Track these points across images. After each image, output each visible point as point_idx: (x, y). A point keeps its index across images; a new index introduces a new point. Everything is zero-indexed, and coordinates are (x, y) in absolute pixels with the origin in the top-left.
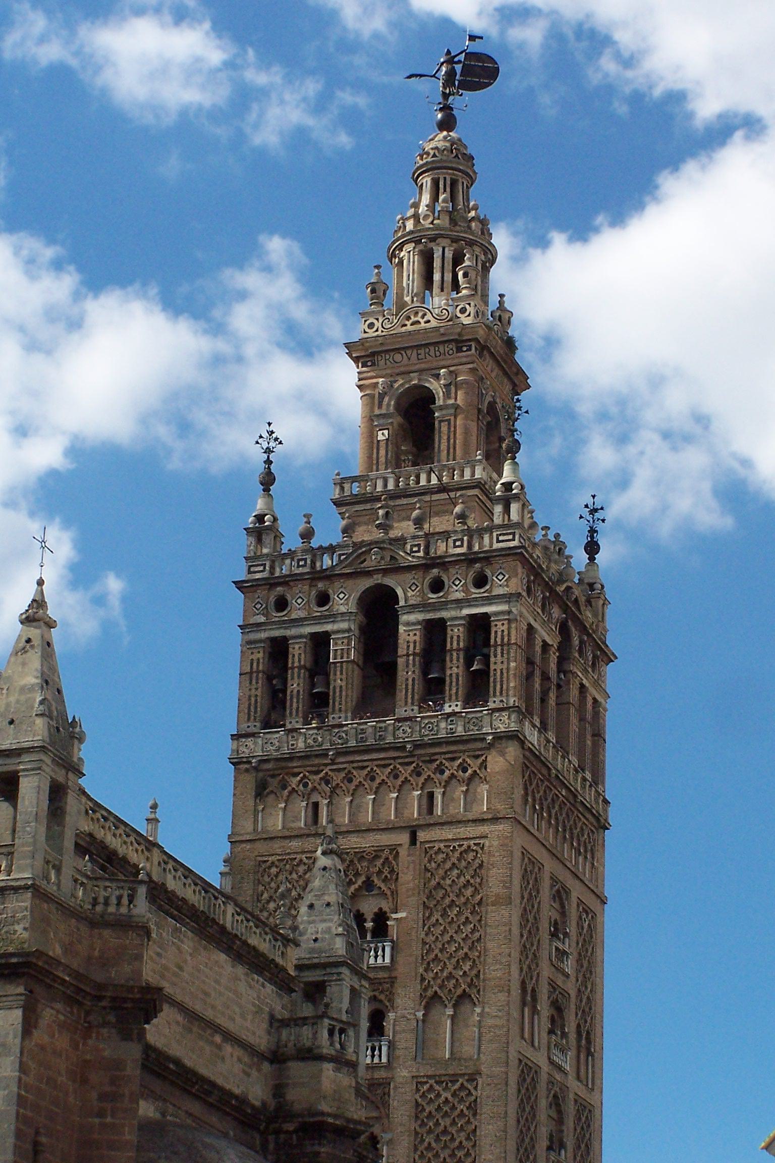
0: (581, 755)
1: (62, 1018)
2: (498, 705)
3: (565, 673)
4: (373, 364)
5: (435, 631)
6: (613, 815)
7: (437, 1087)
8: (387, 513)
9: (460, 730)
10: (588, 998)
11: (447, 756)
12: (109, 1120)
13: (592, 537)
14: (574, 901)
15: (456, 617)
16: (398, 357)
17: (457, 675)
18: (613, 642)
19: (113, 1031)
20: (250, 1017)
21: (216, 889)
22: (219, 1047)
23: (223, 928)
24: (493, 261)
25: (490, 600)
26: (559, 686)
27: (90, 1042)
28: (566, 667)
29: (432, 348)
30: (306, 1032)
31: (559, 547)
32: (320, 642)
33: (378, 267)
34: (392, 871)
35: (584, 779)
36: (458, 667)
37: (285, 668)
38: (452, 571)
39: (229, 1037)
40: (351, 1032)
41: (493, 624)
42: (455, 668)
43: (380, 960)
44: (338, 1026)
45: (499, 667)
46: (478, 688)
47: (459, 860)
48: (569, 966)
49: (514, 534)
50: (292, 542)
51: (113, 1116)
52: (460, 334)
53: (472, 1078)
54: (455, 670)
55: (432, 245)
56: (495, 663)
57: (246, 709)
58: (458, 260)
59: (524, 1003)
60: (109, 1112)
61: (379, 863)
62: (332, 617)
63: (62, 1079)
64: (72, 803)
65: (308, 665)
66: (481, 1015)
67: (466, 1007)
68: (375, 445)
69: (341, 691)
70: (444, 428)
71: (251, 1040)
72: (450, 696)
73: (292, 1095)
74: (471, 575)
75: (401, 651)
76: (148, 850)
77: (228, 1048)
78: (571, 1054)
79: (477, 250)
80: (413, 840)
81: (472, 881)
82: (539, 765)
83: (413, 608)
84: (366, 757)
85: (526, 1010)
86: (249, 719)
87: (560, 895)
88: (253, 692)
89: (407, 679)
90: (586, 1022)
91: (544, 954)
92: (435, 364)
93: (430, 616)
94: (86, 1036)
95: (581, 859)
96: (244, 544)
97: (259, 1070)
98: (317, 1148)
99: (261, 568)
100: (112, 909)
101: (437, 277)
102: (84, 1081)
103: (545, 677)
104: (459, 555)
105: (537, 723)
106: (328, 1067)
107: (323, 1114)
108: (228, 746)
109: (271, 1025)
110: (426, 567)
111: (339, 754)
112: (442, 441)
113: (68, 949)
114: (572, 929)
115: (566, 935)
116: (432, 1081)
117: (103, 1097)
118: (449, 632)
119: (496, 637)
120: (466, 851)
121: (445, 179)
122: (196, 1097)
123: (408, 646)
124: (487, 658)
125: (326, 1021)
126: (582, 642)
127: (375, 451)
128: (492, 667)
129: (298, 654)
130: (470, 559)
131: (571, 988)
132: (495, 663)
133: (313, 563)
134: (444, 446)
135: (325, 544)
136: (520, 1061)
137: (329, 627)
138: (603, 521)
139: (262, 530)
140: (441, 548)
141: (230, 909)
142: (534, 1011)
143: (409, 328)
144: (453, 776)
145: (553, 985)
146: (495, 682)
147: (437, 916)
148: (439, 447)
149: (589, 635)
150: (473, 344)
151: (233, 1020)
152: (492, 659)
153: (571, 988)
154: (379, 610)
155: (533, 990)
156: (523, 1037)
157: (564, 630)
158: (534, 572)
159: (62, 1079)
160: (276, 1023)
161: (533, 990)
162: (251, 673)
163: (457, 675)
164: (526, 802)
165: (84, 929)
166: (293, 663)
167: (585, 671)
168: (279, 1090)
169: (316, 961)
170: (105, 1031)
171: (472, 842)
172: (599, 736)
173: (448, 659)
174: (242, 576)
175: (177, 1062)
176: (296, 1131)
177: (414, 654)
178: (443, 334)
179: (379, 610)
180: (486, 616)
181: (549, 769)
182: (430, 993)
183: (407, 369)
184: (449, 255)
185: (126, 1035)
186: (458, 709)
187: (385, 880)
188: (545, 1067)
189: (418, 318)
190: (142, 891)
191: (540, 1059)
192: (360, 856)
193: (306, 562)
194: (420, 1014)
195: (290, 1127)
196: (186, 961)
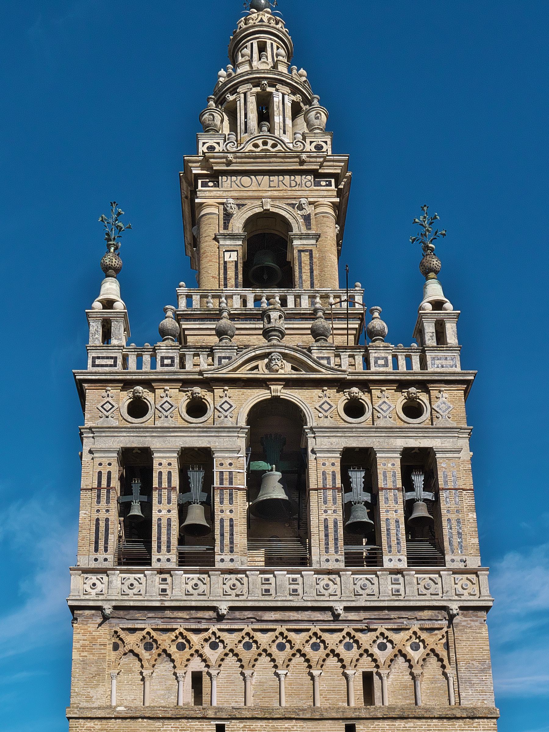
4: (217, 185)
55: (269, 89)
68: (222, 266)
69: (231, 526)
72: (390, 547)
86: (96, 550)
88: (103, 515)
93: (354, 443)
110: (341, 385)
112: (303, 271)
121: (272, 44)
123: (325, 479)
127: (222, 272)
148: (301, 277)
166: (160, 483)
183: (256, 194)
189: (269, 147)
193: (173, 361)
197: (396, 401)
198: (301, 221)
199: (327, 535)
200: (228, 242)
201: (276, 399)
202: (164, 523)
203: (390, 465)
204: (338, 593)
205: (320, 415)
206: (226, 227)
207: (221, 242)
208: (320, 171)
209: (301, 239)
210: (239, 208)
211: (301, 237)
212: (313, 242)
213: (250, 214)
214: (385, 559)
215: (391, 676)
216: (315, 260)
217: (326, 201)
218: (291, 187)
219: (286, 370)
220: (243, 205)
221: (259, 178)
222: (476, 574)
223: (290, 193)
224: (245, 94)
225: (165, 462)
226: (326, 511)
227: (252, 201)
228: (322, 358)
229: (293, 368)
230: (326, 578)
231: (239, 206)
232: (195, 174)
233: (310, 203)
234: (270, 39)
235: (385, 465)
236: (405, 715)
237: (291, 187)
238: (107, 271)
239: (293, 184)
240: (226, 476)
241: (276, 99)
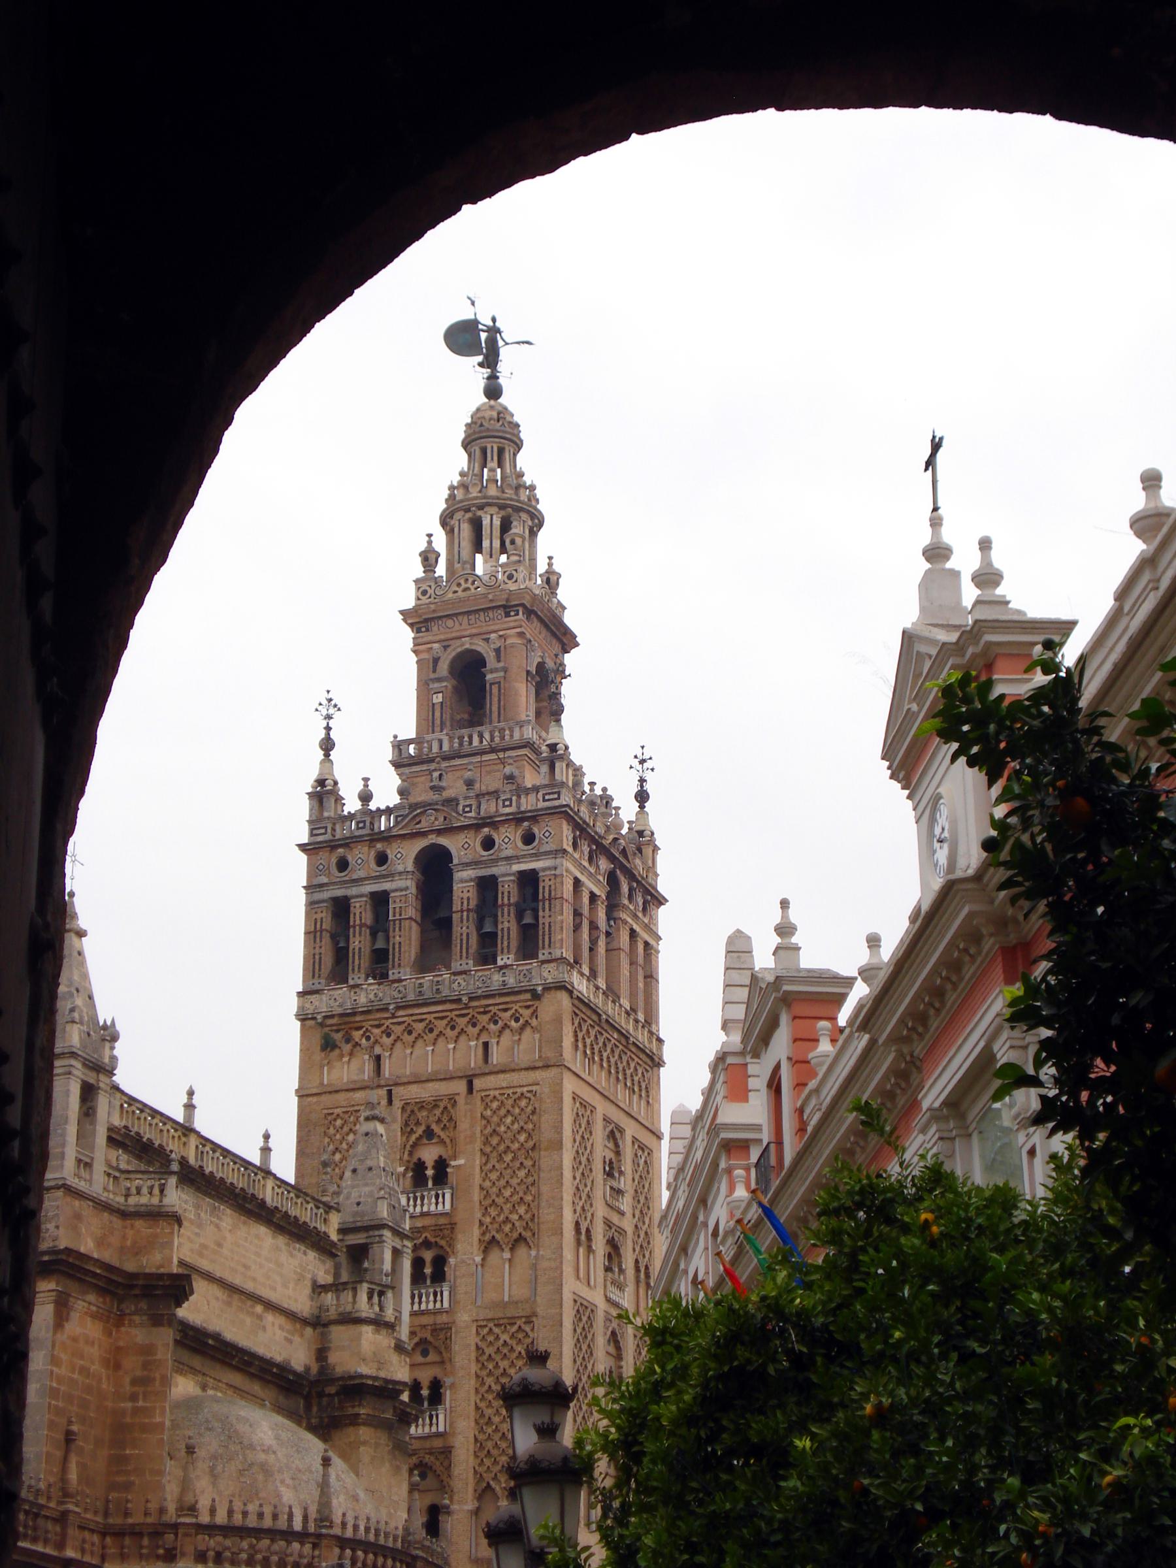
0: (633, 995)
1: (94, 1308)
3: (615, 919)
4: (427, 630)
5: (487, 885)
6: (667, 1053)
7: (496, 1330)
8: (441, 775)
9: (511, 981)
10: (646, 1233)
12: (141, 1403)
13: (642, 786)
14: (629, 1139)
15: (507, 872)
16: (450, 623)
17: (509, 929)
18: (663, 887)
19: (145, 1318)
20: (291, 1286)
21: (255, 1166)
22: (260, 1317)
23: (263, 1202)
24: (540, 525)
25: (537, 856)
26: (608, 934)
27: (123, 1329)
28: (615, 915)
29: (482, 613)
30: (347, 1296)
31: (607, 800)
32: (380, 900)
33: (430, 536)
34: (451, 1119)
35: (637, 1021)
37: (348, 927)
38: (502, 829)
39: (270, 1306)
40: (390, 1294)
42: (507, 924)
43: (440, 1207)
44: (378, 1288)
45: (547, 921)
46: (530, 942)
47: (513, 1107)
48: (626, 1204)
49: (559, 793)
50: (352, 805)
51: (145, 1399)
52: (507, 600)
53: (529, 1321)
54: (506, 925)
55: (480, 513)
57: (312, 966)
58: (506, 526)
59: (578, 1243)
60: (141, 1397)
61: (438, 1112)
62: (390, 876)
63: (95, 1367)
64: (103, 1103)
65: (369, 923)
66: (536, 1257)
67: (522, 1251)
71: (295, 1307)
73: (333, 1358)
74: (520, 832)
75: (456, 906)
76: (185, 1135)
77: (270, 1318)
78: (630, 1289)
79: (524, 516)
80: (470, 1089)
81: (525, 1127)
82: (589, 1013)
84: (425, 1010)
85: (581, 1250)
86: (313, 976)
87: (614, 1135)
88: (317, 951)
90: (644, 1256)
91: (598, 1194)
92: (484, 630)
94: (119, 1323)
95: (635, 1097)
96: (303, 809)
97: (302, 1336)
98: (356, 1410)
99: (323, 831)
100: (144, 1200)
102: (117, 1366)
103: (593, 926)
104: (507, 814)
105: (586, 971)
106: (367, 1331)
107: (361, 1376)
108: (293, 1004)
109: (313, 1291)
110: (477, 827)
111: (398, 1008)
113: (100, 1243)
114: (627, 1166)
115: (621, 1173)
116: (491, 1325)
117: (135, 1382)
118: (500, 888)
120: (519, 1098)
122: (237, 1369)
124: (535, 912)
125: (365, 1286)
126: (631, 890)
128: (541, 921)
129: (361, 913)
130: (518, 819)
131: (628, 1224)
133: (372, 824)
134: (495, 708)
135: (383, 807)
136: (575, 1301)
137: (387, 886)
138: (652, 770)
139: (324, 793)
140: (489, 807)
141: (270, 1183)
142: (590, 1249)
143: (460, 594)
144: (506, 1026)
145: (608, 1224)
146: (544, 935)
147: (493, 1161)
149: (638, 882)
151: (275, 1289)
152: (541, 913)
153: (628, 1224)
154: (435, 868)
155: (588, 1231)
156: (578, 1278)
157: (612, 880)
158: (581, 830)
159: (95, 1367)
160: (318, 1289)
161: (588, 1231)
162: (315, 932)
163: (509, 929)
164: (576, 1047)
165: (117, 1222)
167: (635, 916)
168: (321, 1354)
169: (359, 1224)
170: (137, 1318)
171: (525, 1089)
172: (651, 977)
173: (499, 914)
174: (305, 839)
175: (217, 1337)
176: (337, 1394)
177: (468, 910)
178: (491, 601)
179: (435, 868)
180: (534, 872)
181: (599, 1015)
182: (487, 1237)
183: (458, 634)
184: (497, 522)
185: (157, 1321)
186: (509, 962)
187: (444, 1128)
188: (601, 1305)
189: (469, 585)
190: (173, 1181)
191: (596, 1297)
192: (421, 1105)
194: (478, 1259)
195: (332, 1390)
196: (225, 1238)
200: (436, 685)
202: (357, 951)
206: (434, 671)
212: (502, 674)
213: (454, 654)
214: (499, 959)
221: (460, 618)
225: (358, 905)
230: (463, 976)
231: (446, 647)
240: (397, 910)
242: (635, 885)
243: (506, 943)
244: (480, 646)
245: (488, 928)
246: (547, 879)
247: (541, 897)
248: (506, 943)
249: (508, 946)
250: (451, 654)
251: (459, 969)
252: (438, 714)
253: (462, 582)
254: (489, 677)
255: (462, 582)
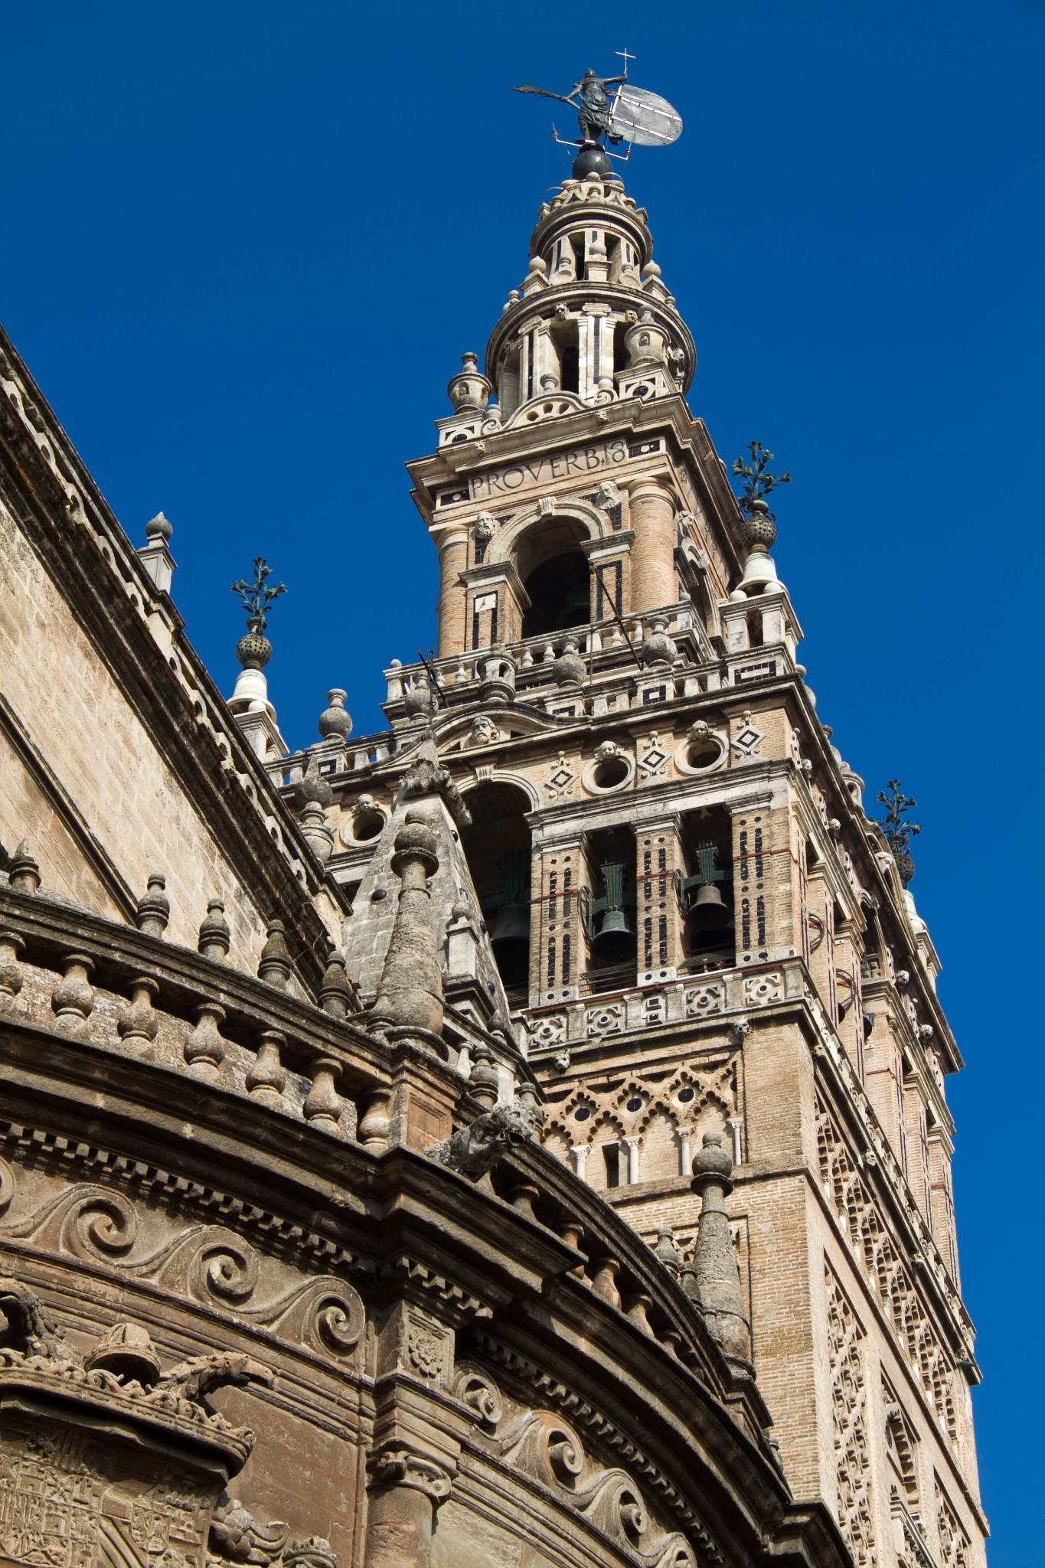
2: (756, 960)
4: (466, 496)
5: (611, 849)
11: (646, 1071)
16: (513, 478)
25: (725, 778)
36: (662, 906)
38: (641, 743)
41: (735, 820)
45: (753, 896)
46: (712, 936)
54: (656, 912)
55: (570, 316)
56: (745, 889)
68: (471, 623)
70: (609, 576)
72: (649, 959)
83: (563, 811)
89: (552, 940)
101: (585, 362)
110: (583, 742)
119: (743, 844)
123: (553, 882)
127: (470, 631)
132: (745, 889)
150: (663, 443)
152: (738, 883)
173: (641, 893)
180: (720, 816)
183: (530, 494)
184: (608, 333)
197: (676, 750)
198: (604, 518)
199: (552, 961)
200: (482, 582)
201: (487, 786)
203: (656, 841)
204: (563, 1038)
205: (552, 793)
206: (479, 558)
207: (471, 585)
208: (635, 430)
209: (602, 548)
210: (502, 524)
211: (602, 544)
212: (625, 547)
213: (521, 527)
215: (647, 1145)
216: (624, 576)
217: (645, 476)
218: (589, 468)
219: (495, 736)
220: (509, 517)
222: (783, 971)
223: (587, 480)
224: (531, 334)
226: (552, 928)
227: (524, 507)
228: (562, 710)
229: (514, 734)
231: (502, 521)
232: (429, 488)
233: (620, 487)
234: (592, 226)
235: (647, 843)
236: (657, 1191)
237: (589, 468)
238: (247, 660)
239: (593, 462)
241: (582, 331)
242: (906, 975)
243: (656, 947)
244: (577, 509)
245: (616, 924)
246: (750, 819)
247: (736, 853)
248: (656, 947)
249: (663, 952)
250: (514, 529)
251: (546, 1002)
252: (485, 630)
253: (539, 410)
254: (595, 556)
255: (539, 410)
